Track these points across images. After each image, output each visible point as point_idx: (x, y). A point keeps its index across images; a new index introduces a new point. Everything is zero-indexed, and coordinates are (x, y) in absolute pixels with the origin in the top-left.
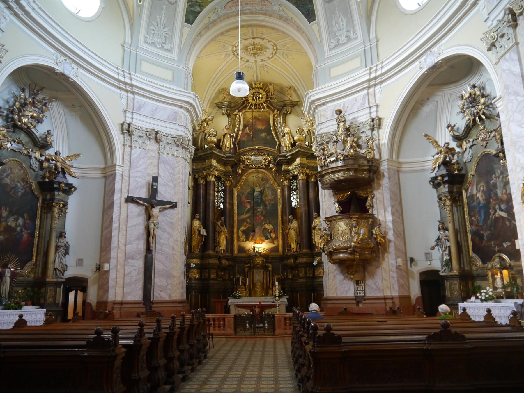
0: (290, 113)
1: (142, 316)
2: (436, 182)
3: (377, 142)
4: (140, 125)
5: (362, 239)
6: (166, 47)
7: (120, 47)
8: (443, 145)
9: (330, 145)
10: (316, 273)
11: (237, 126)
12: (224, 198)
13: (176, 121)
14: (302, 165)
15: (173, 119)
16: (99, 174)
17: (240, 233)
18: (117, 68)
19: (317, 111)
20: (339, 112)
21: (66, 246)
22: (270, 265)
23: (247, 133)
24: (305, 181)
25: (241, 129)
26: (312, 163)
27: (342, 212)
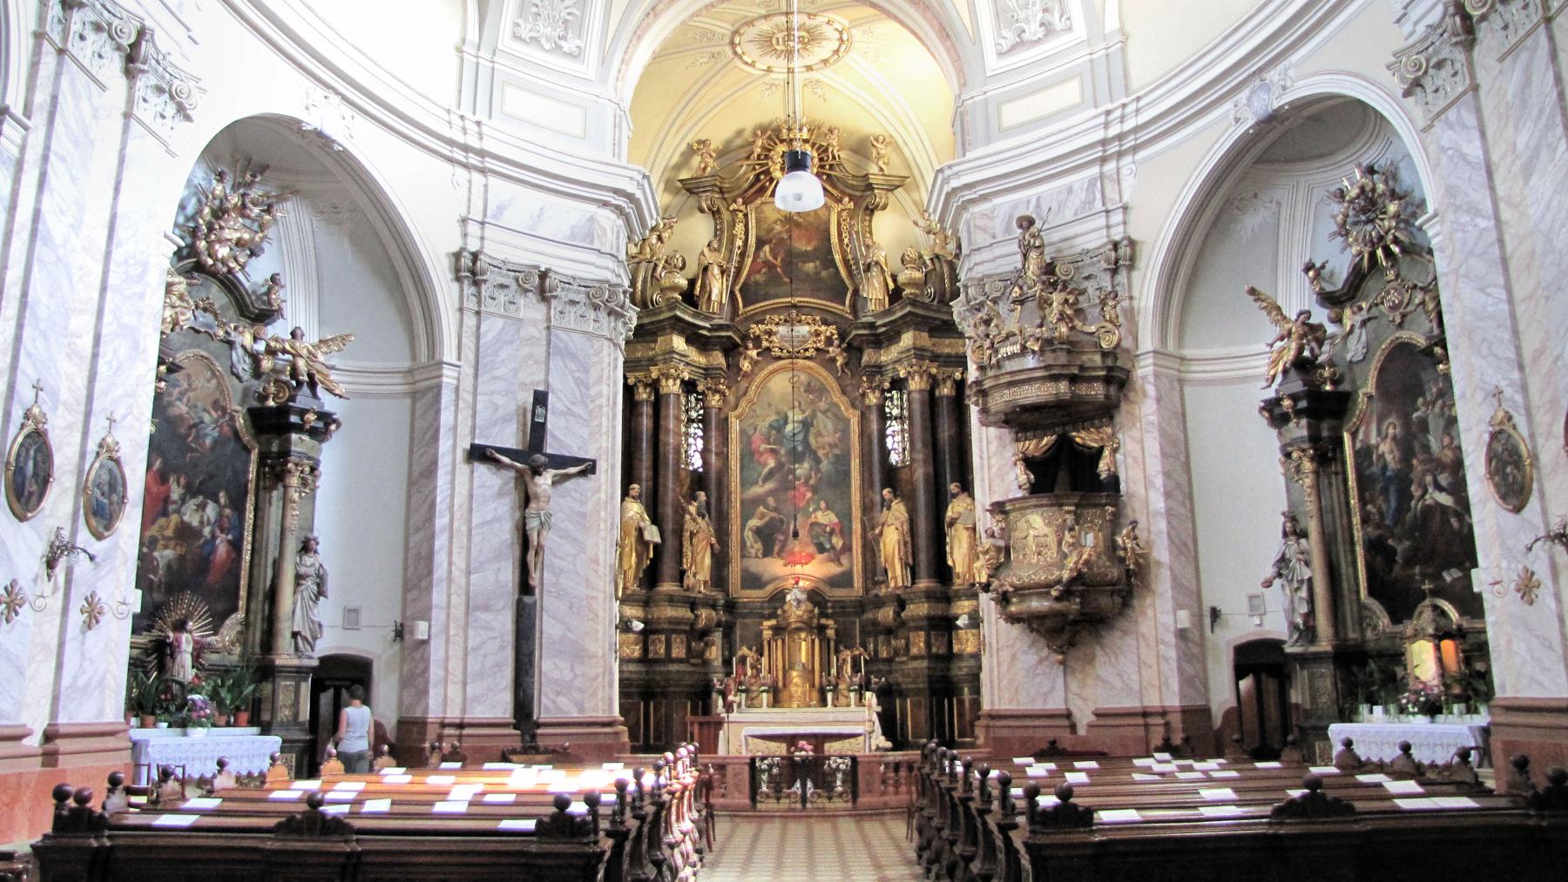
0: (884, 208)
1: (514, 758)
2: (1277, 411)
3: (1125, 303)
4: (501, 257)
5: (1087, 562)
6: (566, 46)
7: (453, 53)
8: (1294, 317)
9: (1003, 308)
10: (956, 649)
11: (739, 243)
12: (706, 438)
13: (592, 242)
14: (919, 353)
15: (585, 239)
16: (397, 385)
17: (749, 535)
18: (449, 111)
19: (966, 216)
20: (1027, 223)
21: (318, 576)
22: (831, 622)
23: (766, 263)
24: (927, 396)
26: (946, 347)
27: (1035, 489)
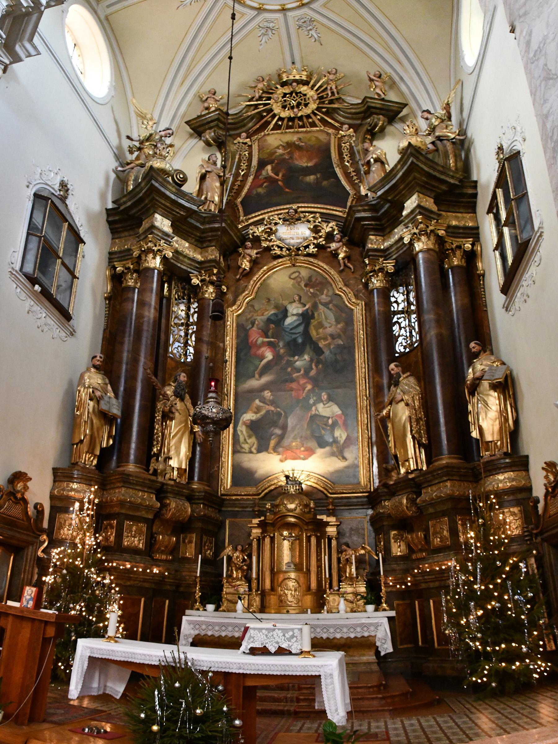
22: (332, 520)
23: (268, 179)
25: (253, 170)
